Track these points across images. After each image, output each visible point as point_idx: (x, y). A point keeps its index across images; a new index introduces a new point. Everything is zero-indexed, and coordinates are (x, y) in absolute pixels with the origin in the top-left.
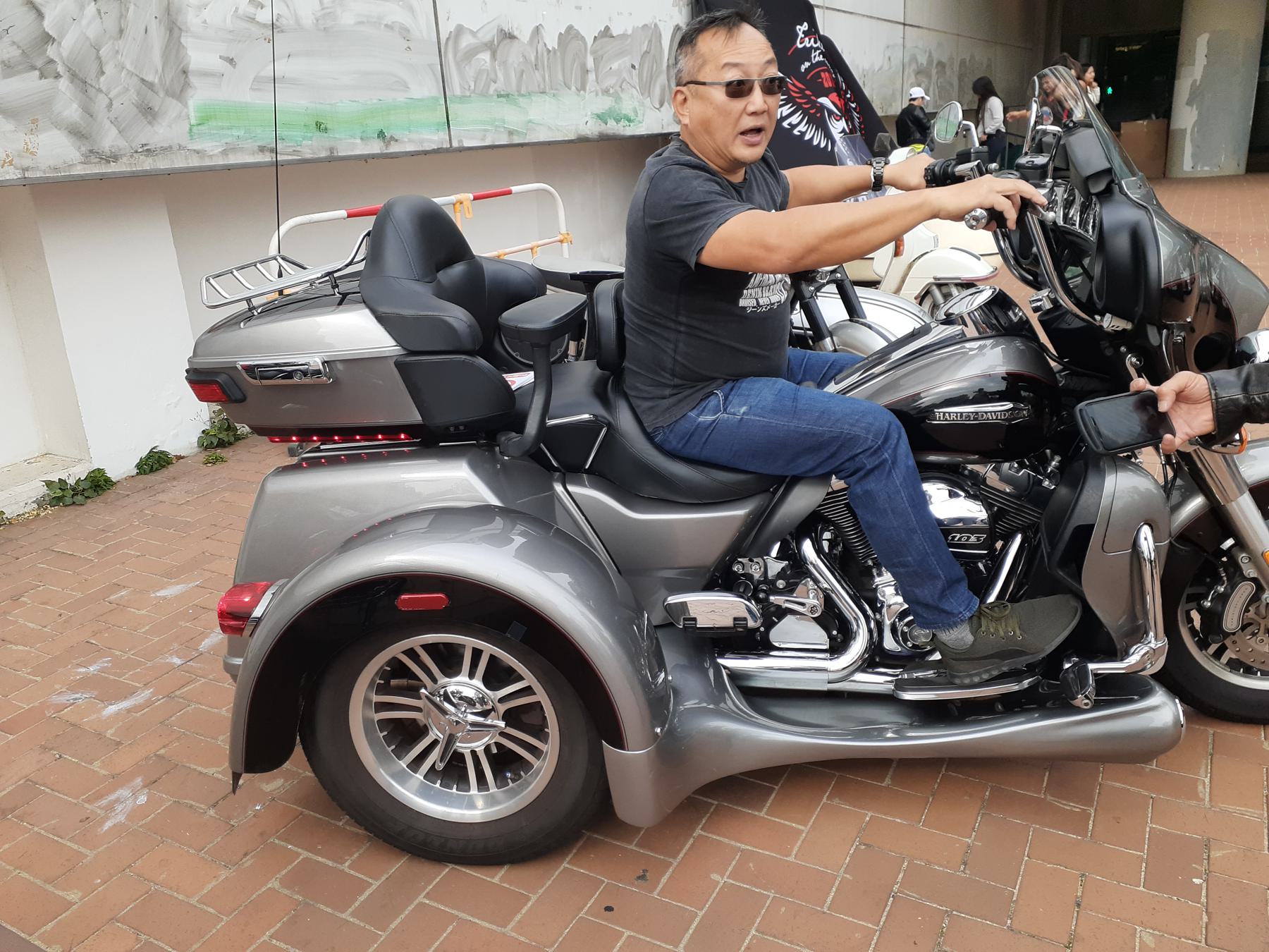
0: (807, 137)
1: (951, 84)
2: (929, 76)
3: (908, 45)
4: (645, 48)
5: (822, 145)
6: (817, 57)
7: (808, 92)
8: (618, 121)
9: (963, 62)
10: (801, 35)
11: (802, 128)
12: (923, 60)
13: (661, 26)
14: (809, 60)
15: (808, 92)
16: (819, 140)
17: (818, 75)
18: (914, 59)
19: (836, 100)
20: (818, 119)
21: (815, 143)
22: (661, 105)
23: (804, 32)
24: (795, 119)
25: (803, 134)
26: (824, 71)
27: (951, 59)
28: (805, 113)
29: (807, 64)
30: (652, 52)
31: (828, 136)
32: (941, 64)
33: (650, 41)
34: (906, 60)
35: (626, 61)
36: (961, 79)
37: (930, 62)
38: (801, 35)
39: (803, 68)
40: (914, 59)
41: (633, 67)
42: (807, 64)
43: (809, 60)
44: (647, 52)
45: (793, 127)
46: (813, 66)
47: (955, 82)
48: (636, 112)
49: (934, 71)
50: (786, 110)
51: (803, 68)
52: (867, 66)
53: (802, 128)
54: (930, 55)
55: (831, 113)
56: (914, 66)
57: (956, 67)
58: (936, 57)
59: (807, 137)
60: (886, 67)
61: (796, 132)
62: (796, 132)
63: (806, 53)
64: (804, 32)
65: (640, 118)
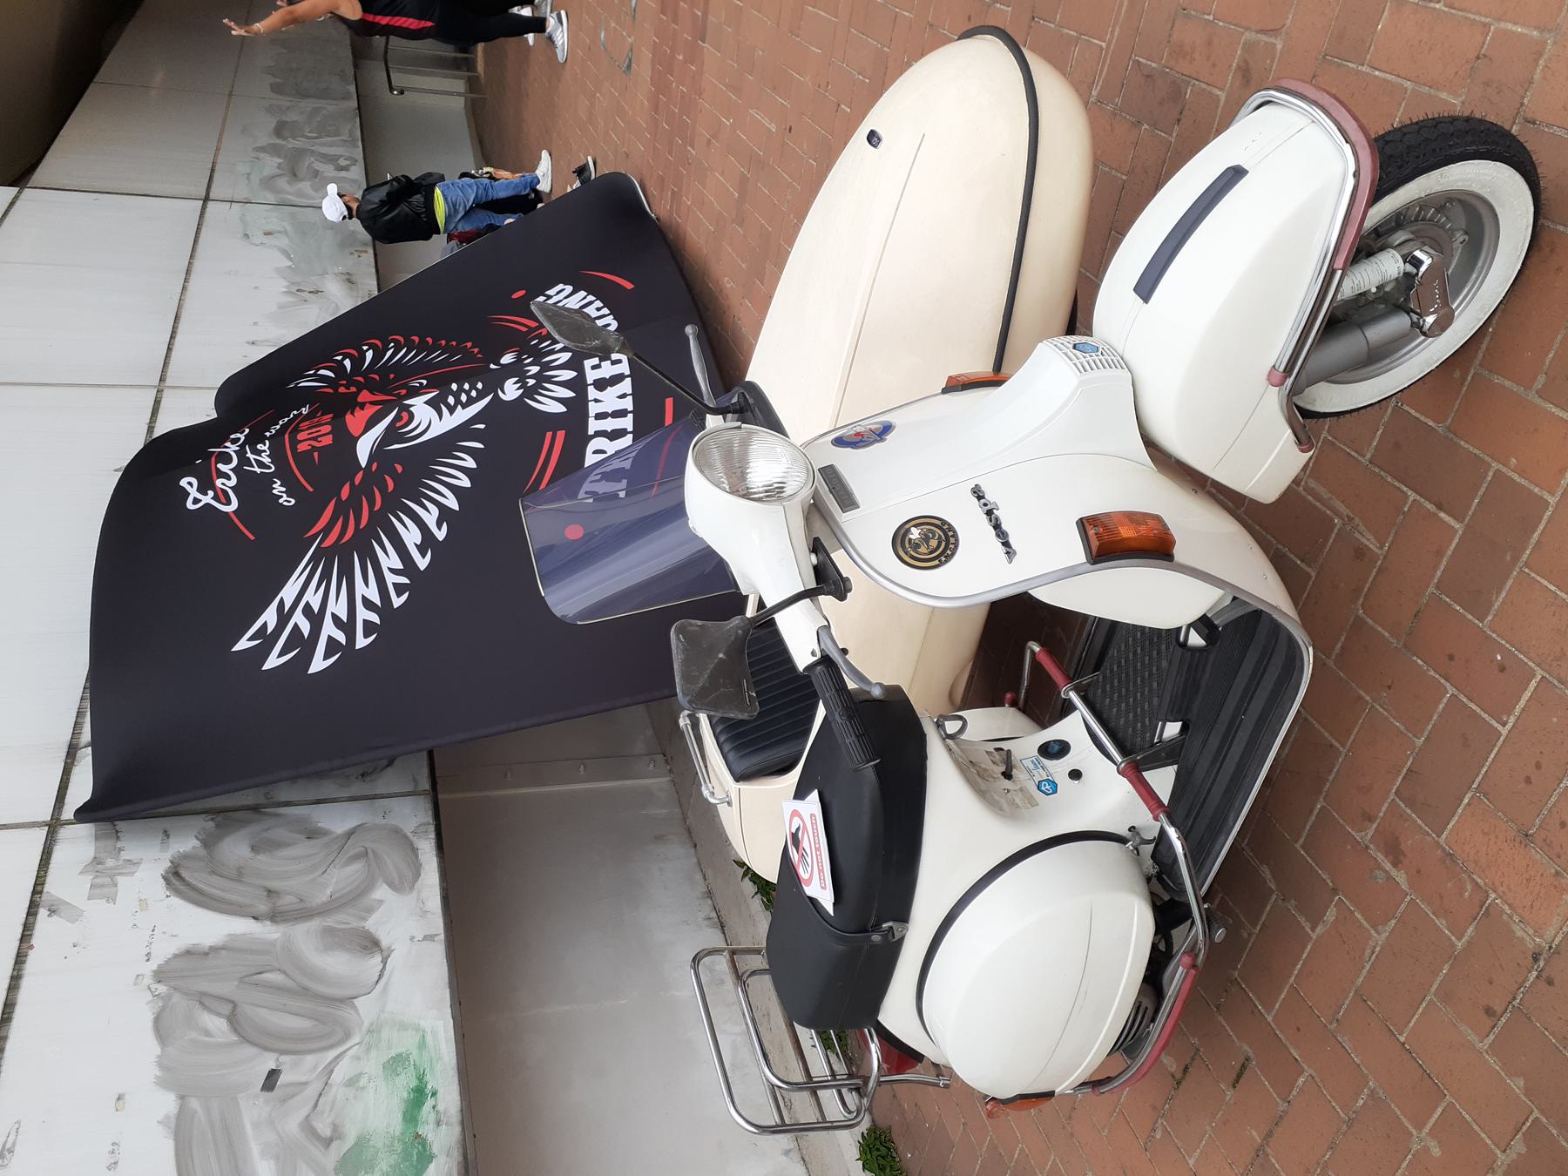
0: (452, 502)
1: (316, 111)
2: (298, 154)
3: (242, 193)
4: (217, 1024)
5: (470, 463)
6: (263, 458)
7: (345, 492)
8: (425, 1157)
9: (277, 89)
10: (208, 499)
11: (430, 517)
12: (271, 164)
13: (165, 950)
14: (267, 480)
15: (345, 492)
16: (460, 471)
17: (303, 459)
18: (268, 183)
19: (362, 416)
20: (411, 467)
21: (465, 482)
22: (370, 944)
23: (202, 490)
24: (411, 536)
25: (445, 514)
26: (294, 443)
27: (270, 110)
28: (394, 505)
29: (278, 488)
30: (227, 988)
31: (447, 444)
32: (279, 130)
33: (204, 1000)
34: (271, 198)
35: (253, 1109)
36: (305, 95)
37: (274, 150)
38: (208, 499)
39: (287, 501)
40: (268, 183)
41: (273, 1075)
42: (278, 488)
43: (267, 480)
44: (233, 1020)
45: (428, 541)
46: (283, 473)
47: (308, 104)
48: (395, 1064)
49: (292, 144)
50: (390, 560)
51: (287, 501)
52: (281, 285)
53: (430, 517)
54: (262, 149)
55: (391, 434)
56: (282, 183)
57: (284, 101)
58: (265, 139)
59: (452, 502)
60: (284, 242)
61: (441, 535)
62: (441, 535)
63: (251, 487)
64: (202, 490)
65: (406, 1043)
